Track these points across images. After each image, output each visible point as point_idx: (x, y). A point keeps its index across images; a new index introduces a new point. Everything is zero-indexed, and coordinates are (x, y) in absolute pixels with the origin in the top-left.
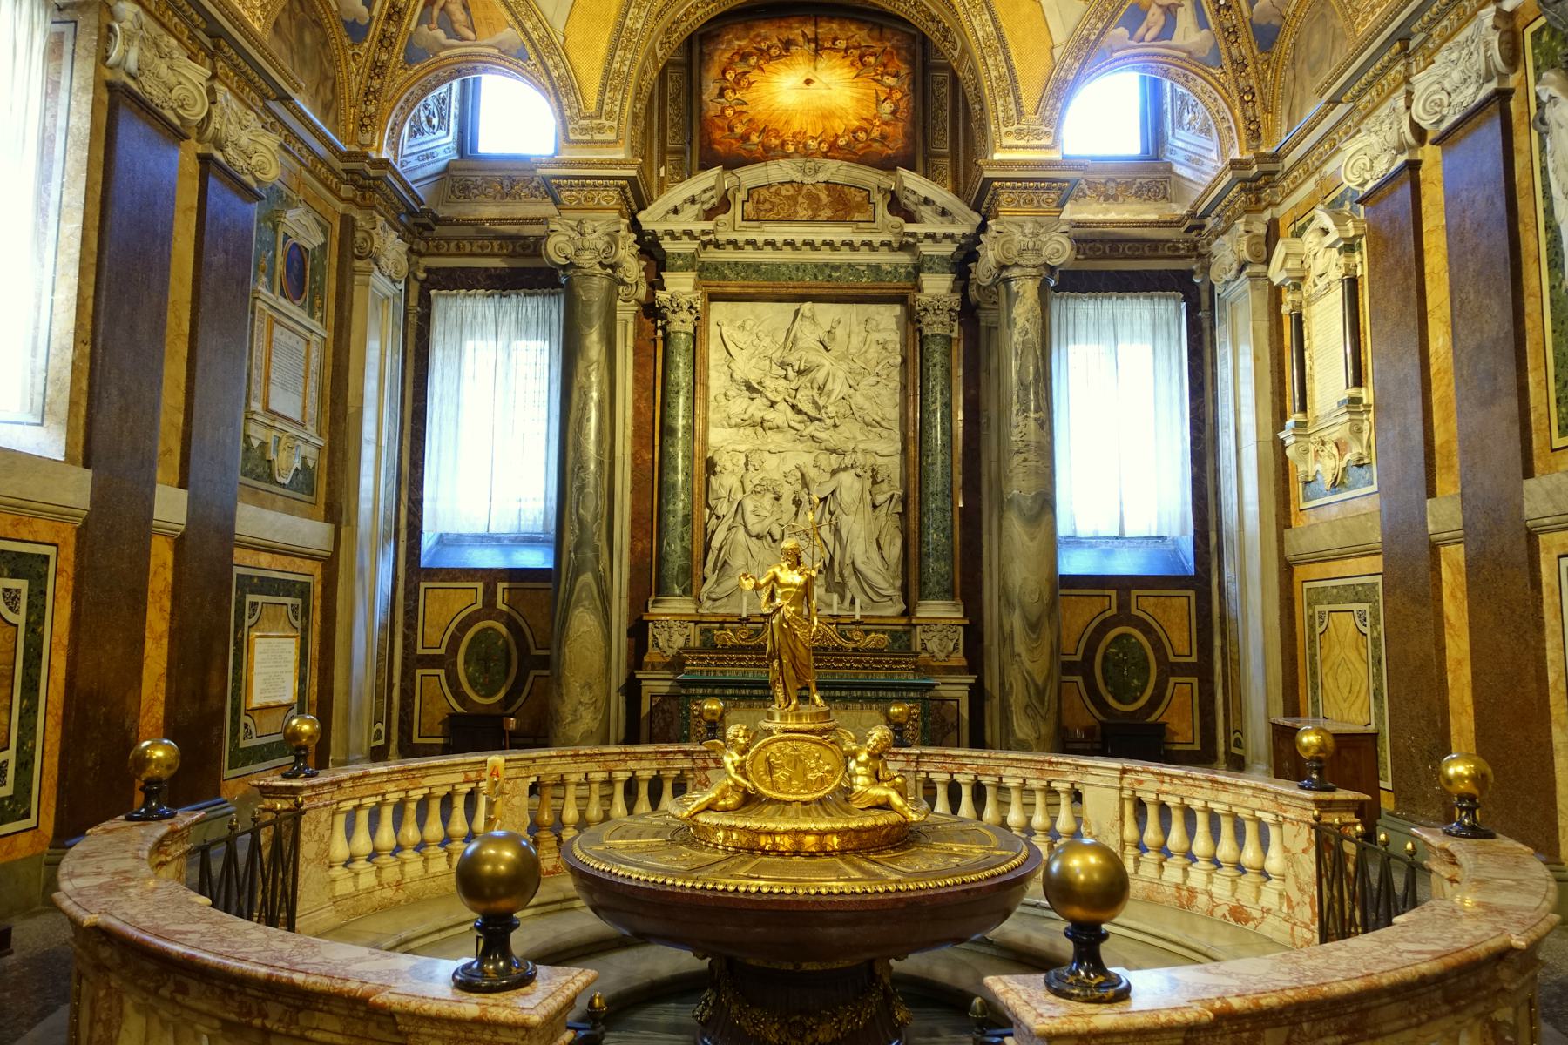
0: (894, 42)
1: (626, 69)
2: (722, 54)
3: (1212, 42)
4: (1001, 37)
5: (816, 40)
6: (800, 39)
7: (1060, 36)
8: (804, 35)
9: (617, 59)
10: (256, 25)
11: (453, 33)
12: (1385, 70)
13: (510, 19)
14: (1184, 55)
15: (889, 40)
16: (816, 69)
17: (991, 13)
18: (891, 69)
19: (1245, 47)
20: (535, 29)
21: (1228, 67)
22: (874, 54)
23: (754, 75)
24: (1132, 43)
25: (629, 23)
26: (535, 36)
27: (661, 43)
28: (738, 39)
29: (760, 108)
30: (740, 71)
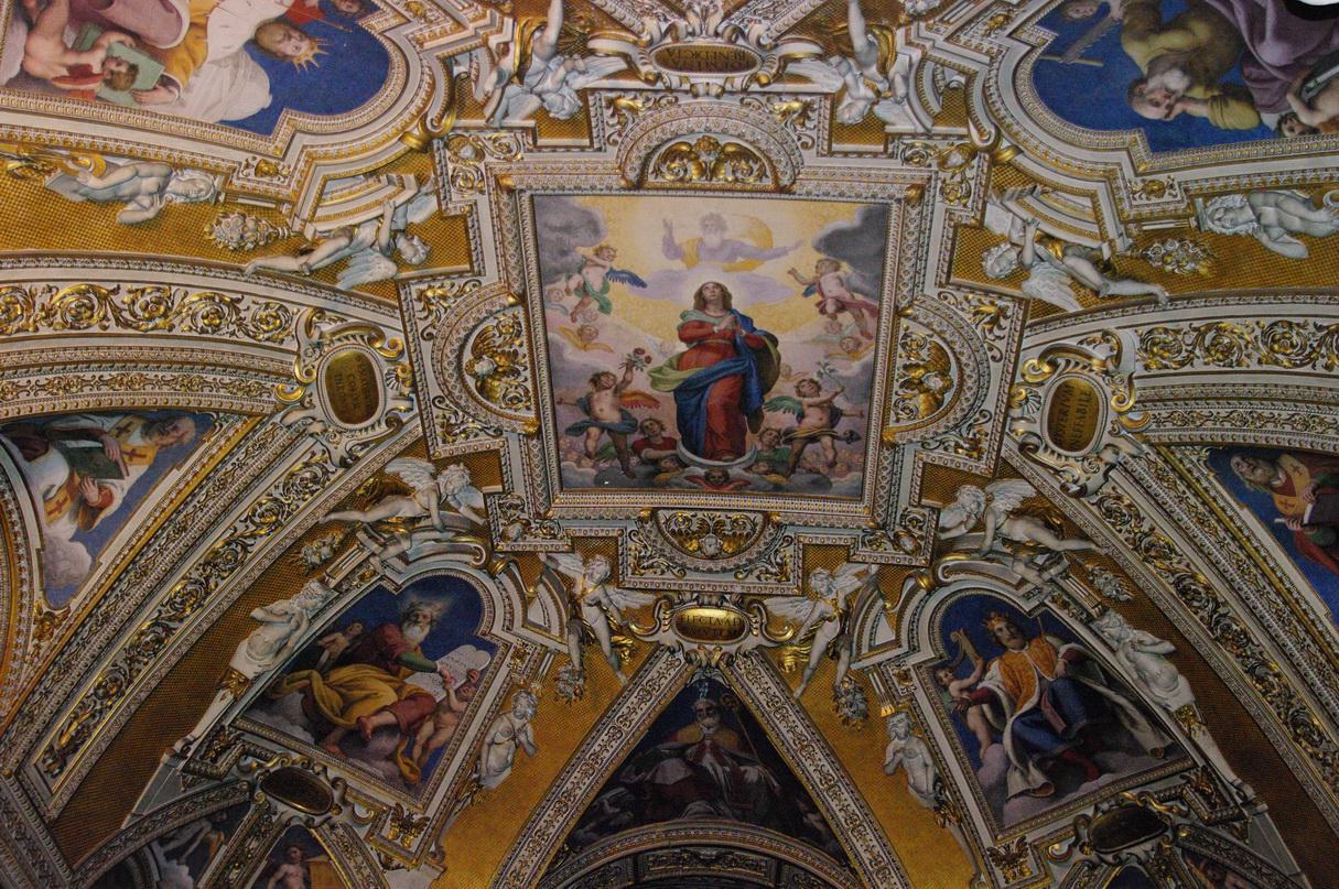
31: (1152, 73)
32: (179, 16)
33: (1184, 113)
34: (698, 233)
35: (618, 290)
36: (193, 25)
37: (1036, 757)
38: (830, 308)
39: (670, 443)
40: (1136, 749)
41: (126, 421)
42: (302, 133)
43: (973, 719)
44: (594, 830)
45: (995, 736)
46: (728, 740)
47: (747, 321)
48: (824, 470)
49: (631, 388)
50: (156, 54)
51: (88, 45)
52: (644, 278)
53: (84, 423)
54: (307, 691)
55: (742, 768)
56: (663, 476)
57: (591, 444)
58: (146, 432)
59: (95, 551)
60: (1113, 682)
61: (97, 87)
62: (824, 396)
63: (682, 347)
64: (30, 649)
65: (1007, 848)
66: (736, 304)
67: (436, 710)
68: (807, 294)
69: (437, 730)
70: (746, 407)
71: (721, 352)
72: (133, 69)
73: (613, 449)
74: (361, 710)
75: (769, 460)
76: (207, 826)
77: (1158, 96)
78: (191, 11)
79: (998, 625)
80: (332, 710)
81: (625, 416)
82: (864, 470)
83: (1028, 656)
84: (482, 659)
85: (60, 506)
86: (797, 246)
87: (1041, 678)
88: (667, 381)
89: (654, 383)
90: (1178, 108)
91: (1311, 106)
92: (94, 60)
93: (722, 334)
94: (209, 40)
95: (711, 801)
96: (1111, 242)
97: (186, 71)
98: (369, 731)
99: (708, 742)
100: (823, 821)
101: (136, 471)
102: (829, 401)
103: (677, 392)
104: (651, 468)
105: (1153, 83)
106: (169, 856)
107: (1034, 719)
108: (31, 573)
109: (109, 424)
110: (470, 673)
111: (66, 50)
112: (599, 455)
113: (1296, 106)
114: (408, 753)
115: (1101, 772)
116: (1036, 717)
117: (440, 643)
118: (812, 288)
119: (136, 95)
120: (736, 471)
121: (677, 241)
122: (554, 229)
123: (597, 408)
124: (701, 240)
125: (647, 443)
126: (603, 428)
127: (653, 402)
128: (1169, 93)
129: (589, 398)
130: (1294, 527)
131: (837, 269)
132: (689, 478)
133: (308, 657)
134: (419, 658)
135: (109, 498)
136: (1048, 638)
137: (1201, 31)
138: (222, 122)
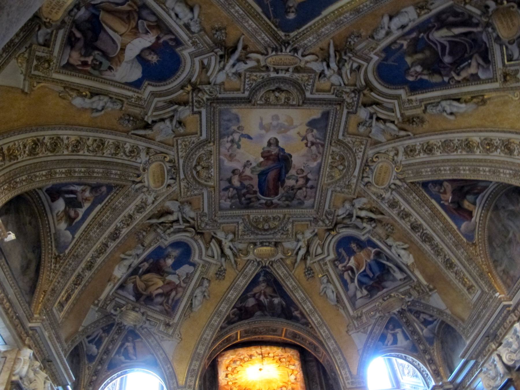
5: (262, 354)
6: (256, 354)
8: (257, 352)
15: (289, 352)
16: (263, 364)
17: (334, 340)
18: (291, 363)
22: (285, 358)
23: (239, 368)
25: (198, 351)
28: (232, 355)
29: (243, 380)
32: (117, 47)
34: (271, 121)
35: (243, 140)
37: (364, 286)
38: (309, 145)
39: (255, 192)
40: (394, 280)
43: (346, 276)
45: (352, 280)
46: (269, 291)
47: (283, 150)
48: (302, 198)
49: (244, 174)
52: (252, 136)
53: (72, 188)
54: (135, 283)
55: (273, 299)
56: (252, 204)
57: (230, 194)
58: (91, 192)
59: (73, 233)
60: (388, 259)
61: (89, 68)
62: (305, 174)
63: (262, 159)
64: (53, 267)
65: (358, 315)
66: (280, 144)
67: (176, 287)
68: (302, 140)
70: (280, 179)
71: (274, 160)
73: (236, 195)
77: (413, 74)
79: (353, 246)
80: (142, 289)
81: (242, 183)
82: (315, 198)
83: (362, 254)
84: (191, 269)
85: (62, 218)
86: (301, 124)
87: (366, 261)
88: (256, 171)
89: (252, 172)
90: (419, 77)
91: (458, 74)
92: (89, 60)
93: (275, 154)
97: (117, 65)
98: (154, 296)
99: (263, 292)
100: (302, 313)
101: (87, 205)
102: (306, 176)
104: (248, 201)
105: (412, 69)
106: (90, 342)
107: (364, 274)
108: (51, 242)
109: (79, 188)
110: (187, 274)
111: (82, 56)
112: (232, 198)
113: (454, 75)
114: (167, 302)
116: (365, 273)
117: (177, 265)
118: (305, 138)
120: (275, 200)
121: (264, 124)
122: (225, 120)
125: (248, 192)
127: (251, 179)
128: (416, 72)
130: (446, 204)
131: (312, 131)
132: (260, 204)
133: (135, 272)
134: (171, 270)
135: (77, 215)
136: (369, 248)
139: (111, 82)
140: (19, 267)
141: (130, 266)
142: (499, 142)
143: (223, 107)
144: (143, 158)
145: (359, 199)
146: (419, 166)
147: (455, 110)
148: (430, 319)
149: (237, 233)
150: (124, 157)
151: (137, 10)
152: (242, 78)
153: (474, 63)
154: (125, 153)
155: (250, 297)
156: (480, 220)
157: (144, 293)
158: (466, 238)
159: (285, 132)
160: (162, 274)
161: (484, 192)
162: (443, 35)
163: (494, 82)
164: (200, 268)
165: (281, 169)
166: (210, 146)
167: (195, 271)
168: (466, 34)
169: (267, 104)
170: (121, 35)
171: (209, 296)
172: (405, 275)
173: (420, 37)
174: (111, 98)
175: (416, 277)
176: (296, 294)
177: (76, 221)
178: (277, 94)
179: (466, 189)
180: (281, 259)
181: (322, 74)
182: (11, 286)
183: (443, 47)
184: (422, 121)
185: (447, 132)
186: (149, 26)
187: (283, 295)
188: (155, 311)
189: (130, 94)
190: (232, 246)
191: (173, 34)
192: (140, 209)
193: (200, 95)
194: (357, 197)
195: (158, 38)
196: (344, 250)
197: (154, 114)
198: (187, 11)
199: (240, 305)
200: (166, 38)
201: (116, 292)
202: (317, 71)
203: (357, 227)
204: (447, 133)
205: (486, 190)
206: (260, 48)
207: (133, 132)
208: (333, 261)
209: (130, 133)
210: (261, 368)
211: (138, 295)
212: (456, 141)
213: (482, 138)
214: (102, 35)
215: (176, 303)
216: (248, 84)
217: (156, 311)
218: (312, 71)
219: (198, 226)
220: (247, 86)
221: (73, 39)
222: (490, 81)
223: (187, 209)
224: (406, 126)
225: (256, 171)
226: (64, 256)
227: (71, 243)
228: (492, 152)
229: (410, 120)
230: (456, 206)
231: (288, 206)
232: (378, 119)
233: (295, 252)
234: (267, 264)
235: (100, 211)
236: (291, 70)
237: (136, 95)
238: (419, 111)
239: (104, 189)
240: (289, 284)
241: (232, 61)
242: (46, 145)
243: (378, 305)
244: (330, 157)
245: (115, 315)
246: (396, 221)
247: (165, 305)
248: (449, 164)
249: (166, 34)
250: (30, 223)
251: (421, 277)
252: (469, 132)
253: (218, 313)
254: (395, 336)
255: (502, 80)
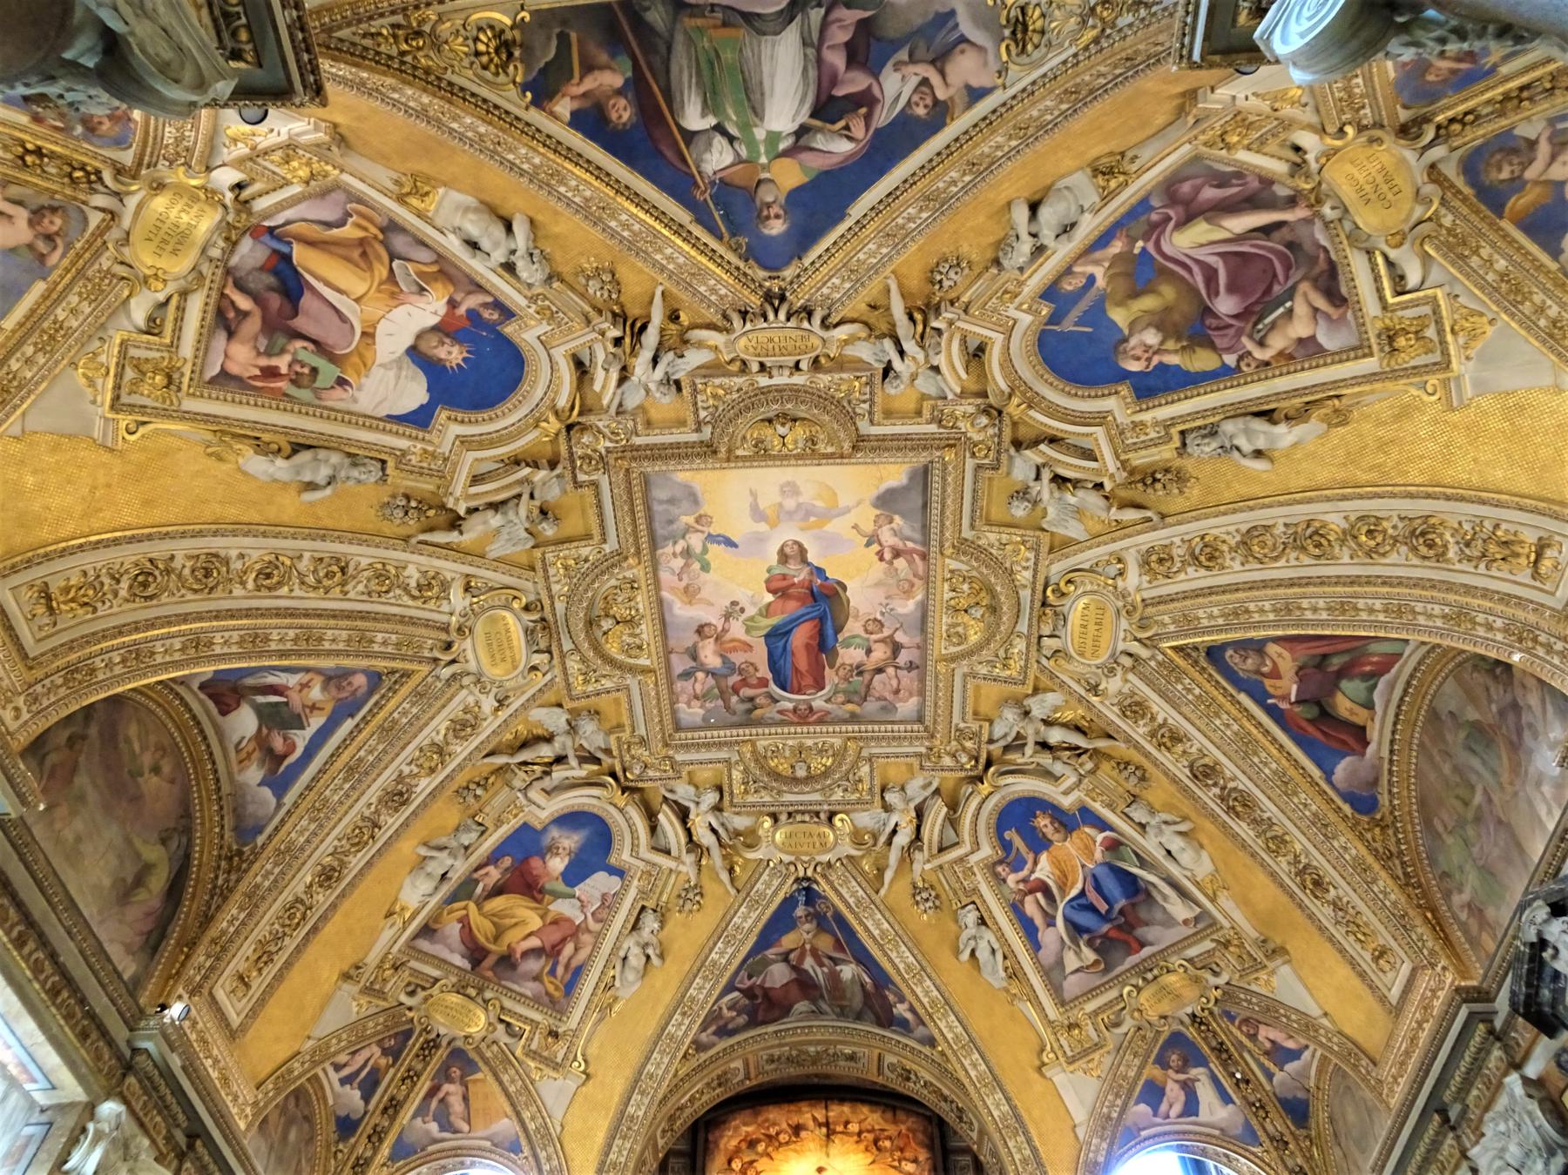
0: (909, 1123)
1: (623, 1160)
2: (730, 1138)
3: (1240, 1120)
4: (1018, 1117)
5: (827, 1124)
6: (811, 1124)
7: (1080, 1115)
8: (815, 1119)
9: (615, 1148)
10: (242, 1125)
11: (446, 1125)
12: (1436, 1145)
13: (508, 1109)
14: (1217, 1132)
15: (903, 1122)
18: (908, 1154)
19: (1278, 1123)
20: (533, 1118)
21: (1267, 1144)
22: (890, 1138)
24: (1158, 1120)
25: (631, 1110)
26: (531, 1126)
27: (664, 1131)
28: (745, 1124)
30: (747, 1159)
31: (1131, 334)
33: (1161, 363)
34: (779, 499)
35: (716, 550)
36: (364, 334)
37: (1086, 937)
38: (888, 556)
39: (763, 683)
40: (1169, 921)
41: (307, 677)
42: (450, 428)
43: (1030, 908)
44: (714, 1033)
45: (1051, 922)
46: (825, 943)
47: (820, 571)
48: (890, 697)
50: (333, 359)
51: (277, 350)
53: (271, 679)
54: (465, 922)
56: (758, 712)
57: (698, 687)
58: (325, 688)
60: (1143, 863)
61: (282, 385)
62: (886, 632)
63: (769, 598)
66: (811, 557)
67: (575, 932)
68: (868, 544)
69: (576, 949)
70: (823, 646)
72: (314, 371)
74: (512, 937)
75: (844, 692)
76: (376, 1051)
77: (1139, 352)
78: (363, 321)
79: (1043, 822)
84: (614, 883)
85: (249, 755)
86: (859, 503)
87: (1083, 866)
88: (758, 628)
89: (748, 631)
90: (1156, 360)
91: (1261, 344)
92: (282, 363)
94: (377, 347)
95: (814, 1001)
96: (1112, 476)
98: (518, 956)
99: (808, 947)
100: (912, 1010)
101: (316, 722)
102: (891, 637)
103: (767, 636)
104: (748, 706)
105: (1133, 342)
106: (343, 1082)
107: (1081, 903)
109: (292, 680)
110: (604, 897)
111: (259, 354)
113: (1249, 345)
114: (553, 972)
115: (1142, 945)
116: (1082, 901)
117: (576, 873)
119: (317, 392)
120: (818, 703)
121: (762, 507)
122: (661, 502)
123: (702, 655)
124: (780, 505)
125: (745, 682)
126: (708, 672)
127: (748, 647)
128: (1147, 348)
129: (695, 646)
130: (1284, 706)
131: (891, 522)
132: (781, 712)
133: (464, 890)
134: (560, 886)
135: (293, 747)
136: (1087, 830)
137: (1168, 292)
138: (389, 416)
139: (347, 417)
140: (107, 882)
141: (444, 875)
142: (1400, 525)
143: (649, 468)
144: (458, 599)
145: (1039, 697)
146: (1188, 603)
147: (1261, 444)
148: (1290, 1044)
149: (726, 788)
150: (406, 600)
151: (381, 237)
152: (686, 391)
153: (1301, 308)
154: (406, 590)
155: (775, 961)
156: (1392, 752)
157: (492, 947)
158: (1353, 806)
159: (819, 525)
160: (539, 896)
161: (1394, 671)
162: (1203, 240)
163: (1365, 356)
164: (635, 882)
165: (822, 619)
166: (630, 567)
167: (625, 888)
168: (1266, 230)
169: (762, 455)
170: (357, 300)
171: (662, 956)
172: (1198, 910)
173: (1136, 251)
174: (349, 455)
175: (1227, 916)
176: (893, 955)
177: (286, 763)
178: (781, 430)
179: (1336, 663)
180: (848, 857)
181: (888, 370)
182: (69, 933)
183: (1210, 275)
184: (1180, 478)
185: (1251, 503)
186: (420, 274)
187: (864, 958)
188: (520, 997)
189: (403, 443)
190: (715, 825)
191: (488, 292)
192: (462, 728)
193: (586, 439)
194: (1036, 690)
195: (453, 304)
196: (1018, 831)
197: (473, 490)
198: (498, 231)
199: (748, 983)
200: (473, 301)
201: (410, 945)
202: (876, 365)
203: (1047, 774)
204: (1251, 509)
205: (1397, 666)
206: (713, 316)
207: (422, 537)
208: (991, 867)
209: (413, 541)
210: (822, 1164)
211: (476, 954)
212: (1282, 529)
213: (1353, 518)
214: (307, 301)
215: (577, 973)
216: (705, 409)
217: (522, 995)
218: (858, 365)
219: (624, 771)
220: (703, 414)
221: (231, 315)
222: (1352, 354)
223: (588, 727)
224: (1137, 493)
225: (758, 628)
226: (253, 852)
227: (271, 819)
228: (1384, 555)
229: (1149, 477)
230: (1313, 712)
231: (854, 718)
232: (1060, 481)
233: (883, 839)
234: (810, 873)
235: (351, 736)
236: (803, 366)
237: (419, 446)
238: (1166, 453)
239: (360, 680)
240: (872, 928)
241: (646, 355)
242: (180, 576)
243: (1129, 994)
244: (946, 586)
245: (410, 1009)
246: (1147, 755)
247: (546, 979)
248: (1270, 592)
249: (469, 293)
250: (156, 770)
251: (1238, 916)
252: (1310, 501)
253: (680, 1003)
254: (1188, 1088)
255: (1387, 349)
